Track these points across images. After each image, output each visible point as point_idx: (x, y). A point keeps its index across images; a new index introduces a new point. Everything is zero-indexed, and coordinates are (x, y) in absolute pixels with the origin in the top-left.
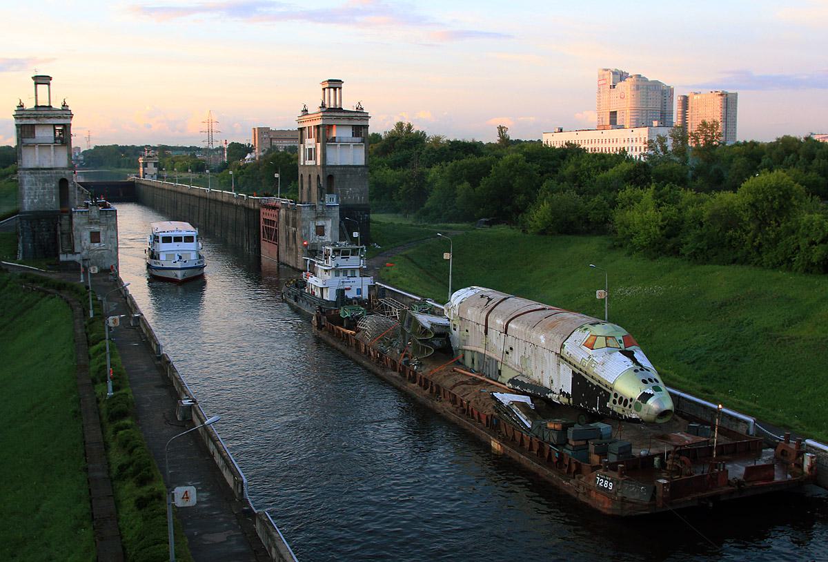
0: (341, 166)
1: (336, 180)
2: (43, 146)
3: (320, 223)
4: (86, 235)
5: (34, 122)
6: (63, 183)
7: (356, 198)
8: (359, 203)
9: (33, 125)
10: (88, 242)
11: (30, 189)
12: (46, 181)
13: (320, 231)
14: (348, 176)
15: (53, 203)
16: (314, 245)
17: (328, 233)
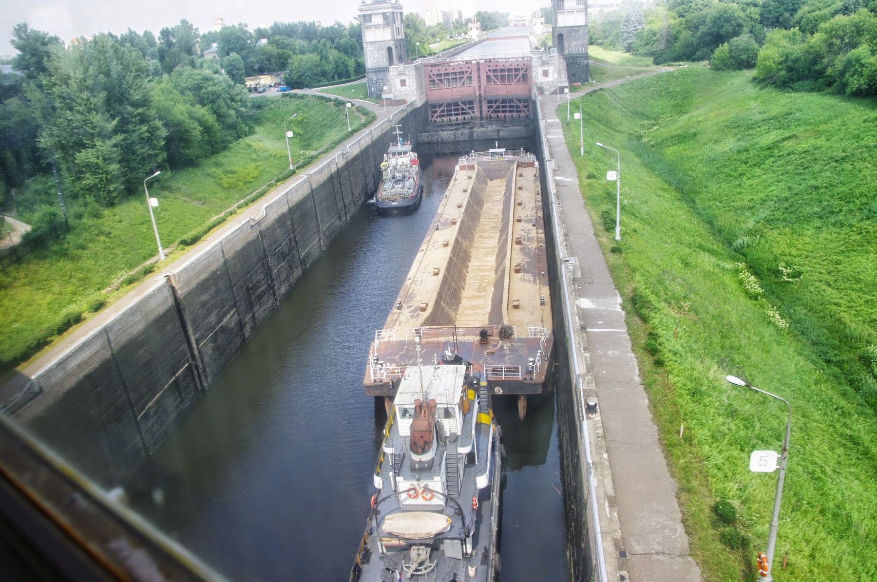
0: (568, 27)
1: (565, 37)
2: (377, 27)
3: (546, 68)
4: (398, 82)
5: (370, 12)
6: (389, 49)
7: (578, 50)
8: (580, 52)
9: (370, 15)
10: (399, 87)
11: (371, 55)
12: (379, 49)
13: (546, 74)
14: (573, 34)
15: (384, 62)
16: (541, 83)
17: (550, 74)
